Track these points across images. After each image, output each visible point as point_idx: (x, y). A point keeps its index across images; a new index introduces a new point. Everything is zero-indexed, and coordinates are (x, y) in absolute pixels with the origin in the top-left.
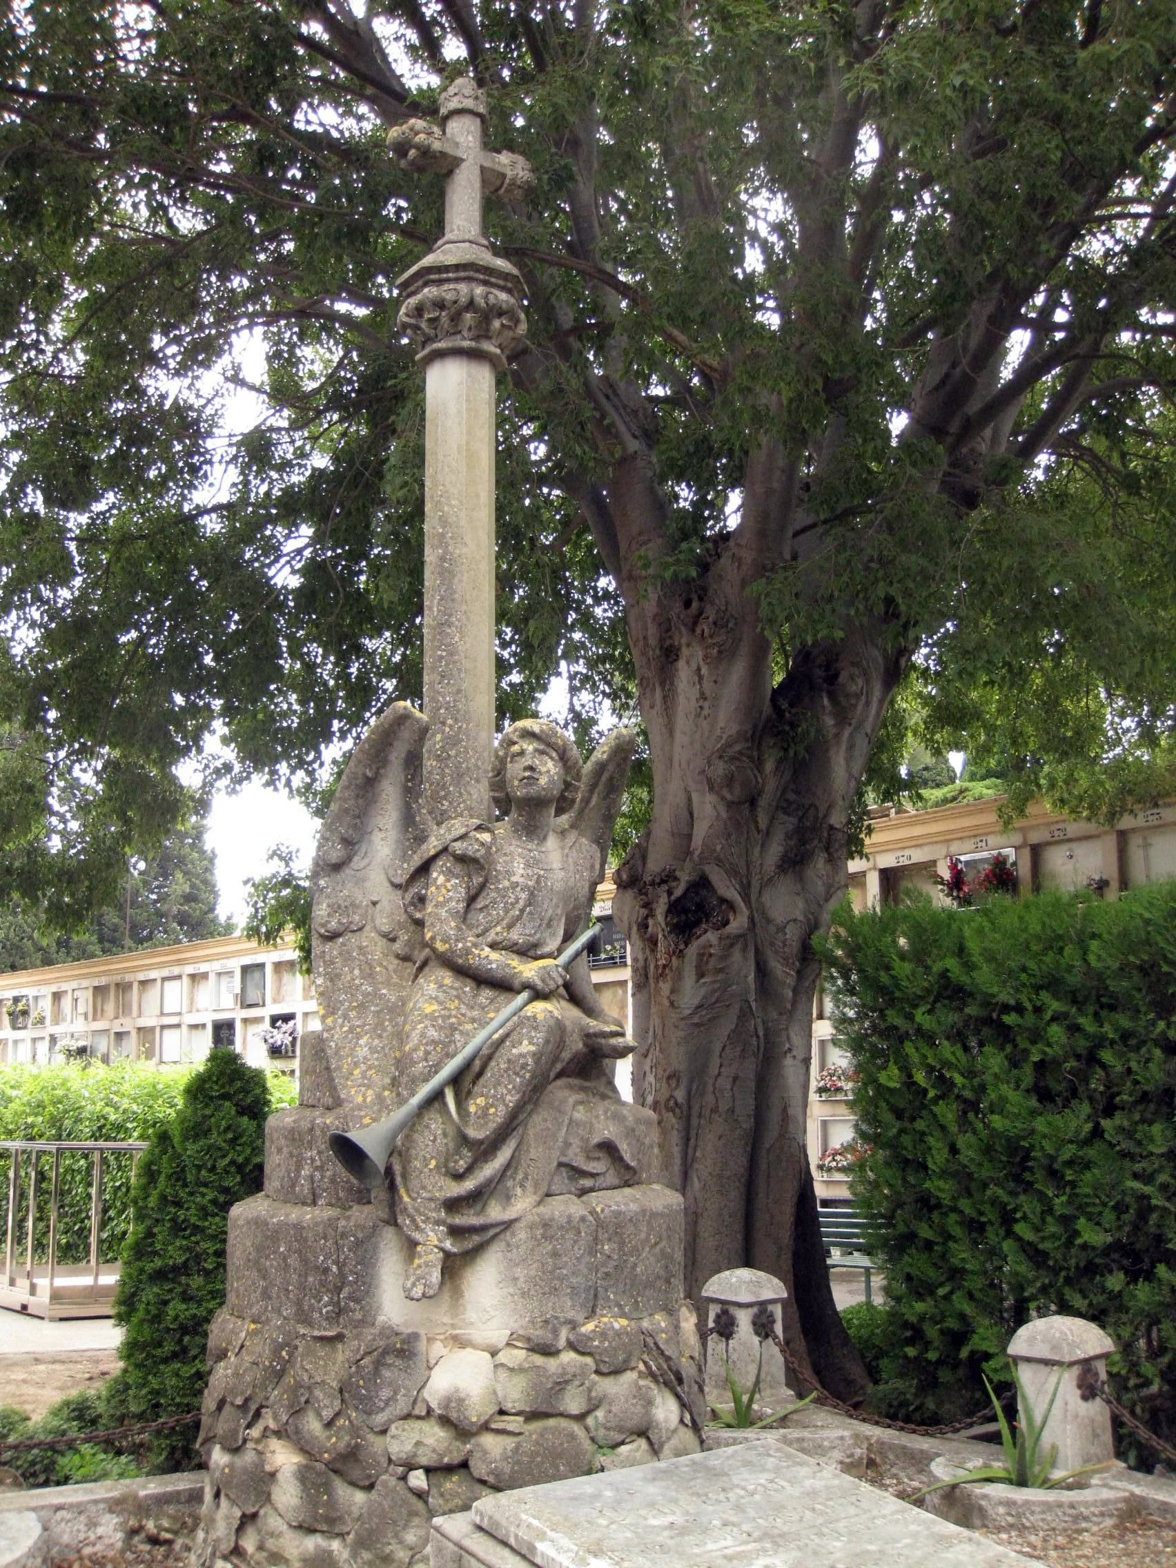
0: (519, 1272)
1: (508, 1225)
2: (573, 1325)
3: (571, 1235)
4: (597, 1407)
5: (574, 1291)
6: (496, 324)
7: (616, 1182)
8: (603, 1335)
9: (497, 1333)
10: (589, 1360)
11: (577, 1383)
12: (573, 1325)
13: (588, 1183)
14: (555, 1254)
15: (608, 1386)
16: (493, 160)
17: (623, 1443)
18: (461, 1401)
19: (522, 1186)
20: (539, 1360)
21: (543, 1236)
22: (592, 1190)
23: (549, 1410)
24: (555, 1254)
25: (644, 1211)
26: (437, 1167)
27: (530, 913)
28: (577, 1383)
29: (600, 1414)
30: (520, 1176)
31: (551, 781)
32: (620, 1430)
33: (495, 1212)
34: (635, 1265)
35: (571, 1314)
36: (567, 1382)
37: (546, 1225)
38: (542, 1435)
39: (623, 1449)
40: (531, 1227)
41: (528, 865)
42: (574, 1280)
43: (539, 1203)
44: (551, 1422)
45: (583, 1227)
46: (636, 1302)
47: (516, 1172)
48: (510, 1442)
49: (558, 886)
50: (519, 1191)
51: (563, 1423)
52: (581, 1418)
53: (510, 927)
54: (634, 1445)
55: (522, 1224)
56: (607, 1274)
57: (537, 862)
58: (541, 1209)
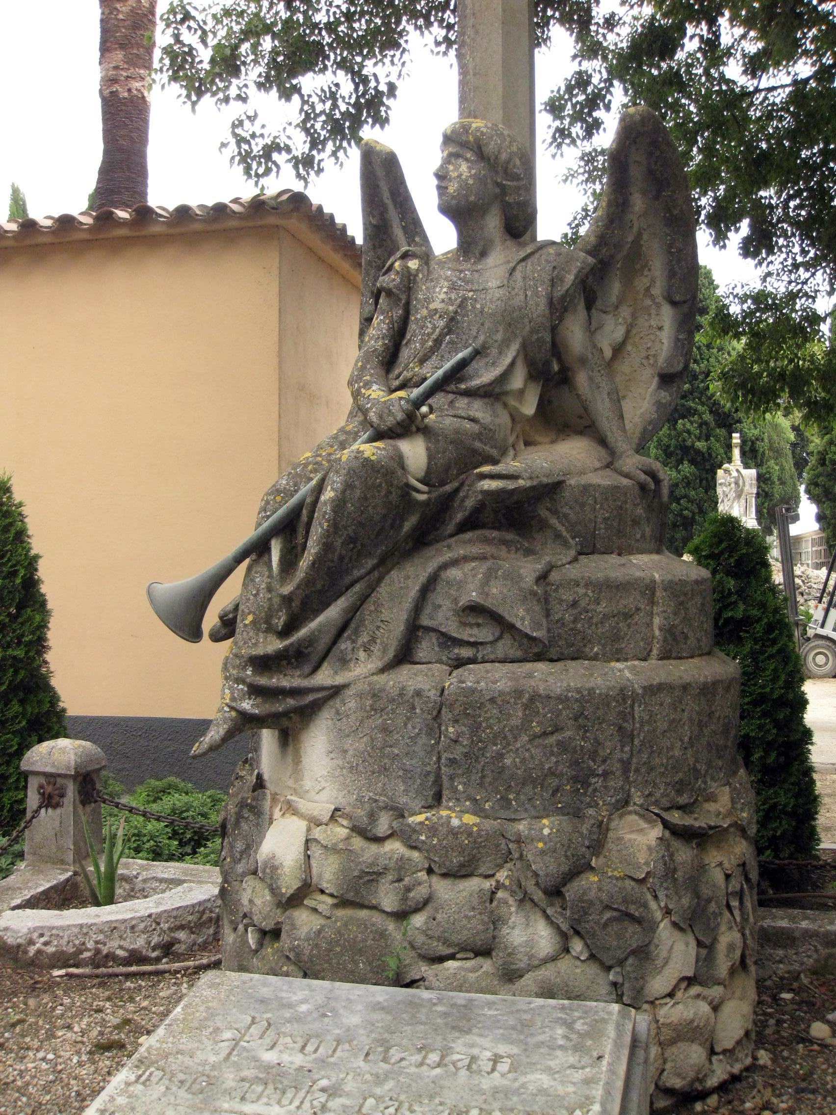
1: (336, 691)
3: (403, 710)
4: (417, 910)
5: (407, 775)
7: (519, 654)
8: (433, 830)
10: (416, 854)
13: (466, 652)
14: (385, 730)
15: (443, 889)
17: (452, 957)
18: (274, 868)
20: (358, 843)
21: (373, 709)
22: (473, 661)
25: (518, 693)
26: (254, 622)
27: (451, 342)
29: (418, 920)
30: (364, 638)
31: (464, 185)
32: (446, 942)
33: (325, 677)
34: (500, 756)
38: (346, 925)
39: (451, 964)
40: (360, 695)
41: (453, 288)
42: (408, 763)
43: (382, 671)
44: (363, 914)
45: (417, 702)
47: (356, 632)
49: (490, 308)
50: (362, 655)
51: (377, 918)
52: (401, 915)
53: (422, 362)
54: (469, 964)
56: (452, 762)
58: (382, 678)
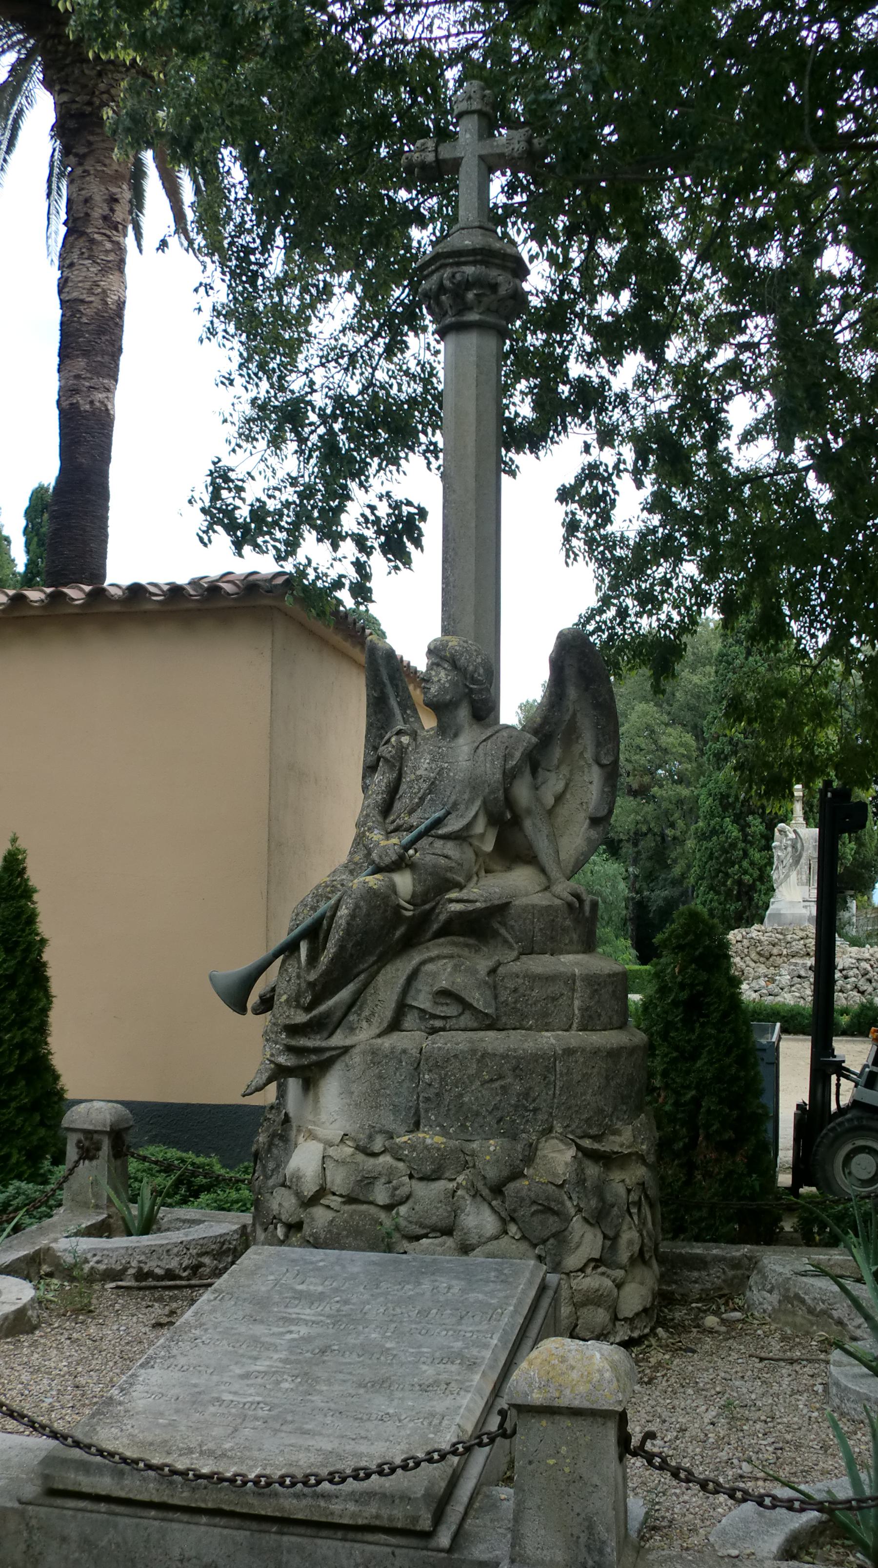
0: (354, 1087)
1: (346, 1050)
2: (391, 1136)
3: (393, 1063)
4: (402, 1203)
5: (396, 1109)
6: (470, 295)
7: (475, 1025)
8: (413, 1148)
9: (333, 1132)
10: (401, 1165)
11: (383, 1180)
12: (391, 1136)
13: (438, 1023)
14: (380, 1077)
15: (420, 1189)
16: (492, 146)
17: (426, 1236)
18: (299, 1178)
19: (368, 1020)
20: (360, 1157)
21: (372, 1062)
22: (443, 1029)
23: (361, 1197)
24: (380, 1077)
25: (474, 1051)
26: (287, 1001)
27: (431, 799)
28: (383, 1180)
29: (403, 1210)
30: (366, 1013)
31: (442, 689)
32: (422, 1226)
33: (338, 1040)
34: (461, 1096)
35: (392, 1127)
36: (375, 1178)
37: (374, 1053)
38: (351, 1216)
39: (424, 1241)
40: (364, 1053)
41: (433, 760)
42: (396, 1100)
43: (379, 1036)
44: (364, 1207)
45: (404, 1058)
46: (463, 1125)
47: (361, 1008)
48: (330, 1215)
49: (460, 776)
50: (364, 1024)
51: (373, 1210)
52: (389, 1208)
53: (410, 813)
54: (437, 1241)
55: (356, 1050)
56: (428, 1099)
57: (443, 756)
58: (379, 1041)
